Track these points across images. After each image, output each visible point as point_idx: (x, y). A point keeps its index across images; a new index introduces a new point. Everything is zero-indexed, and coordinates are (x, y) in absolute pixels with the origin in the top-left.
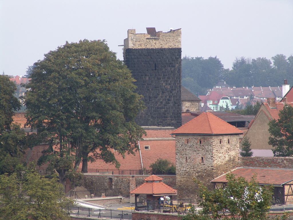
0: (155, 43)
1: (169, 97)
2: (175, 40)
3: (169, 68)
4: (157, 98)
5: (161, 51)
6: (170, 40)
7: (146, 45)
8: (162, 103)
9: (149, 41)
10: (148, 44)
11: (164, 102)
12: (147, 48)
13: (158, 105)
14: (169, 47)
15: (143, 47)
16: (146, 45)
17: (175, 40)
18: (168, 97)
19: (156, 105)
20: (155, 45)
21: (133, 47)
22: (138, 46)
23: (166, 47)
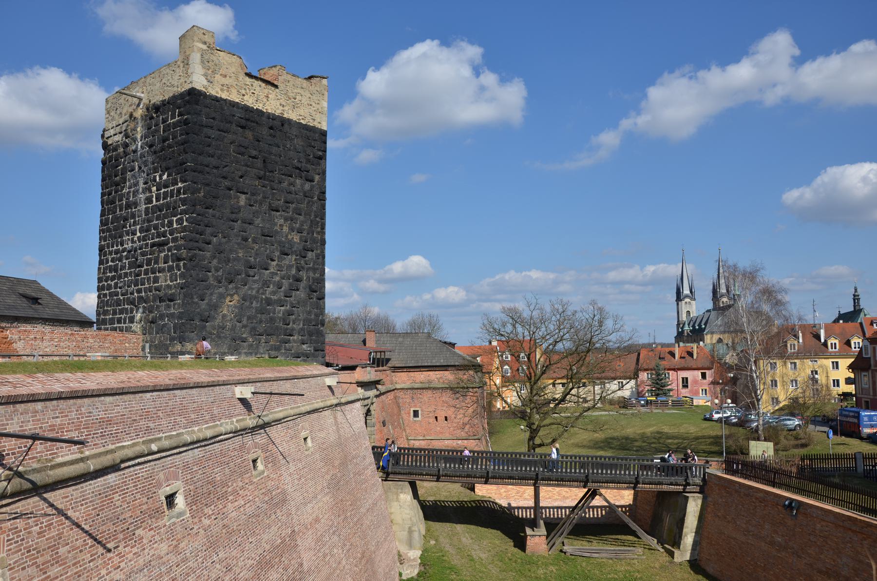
2: (314, 104)
3: (298, 181)
4: (266, 269)
5: (278, 124)
6: (305, 101)
11: (286, 283)
15: (235, 97)
17: (314, 104)
18: (294, 271)
20: (265, 100)
22: (222, 90)
23: (292, 115)
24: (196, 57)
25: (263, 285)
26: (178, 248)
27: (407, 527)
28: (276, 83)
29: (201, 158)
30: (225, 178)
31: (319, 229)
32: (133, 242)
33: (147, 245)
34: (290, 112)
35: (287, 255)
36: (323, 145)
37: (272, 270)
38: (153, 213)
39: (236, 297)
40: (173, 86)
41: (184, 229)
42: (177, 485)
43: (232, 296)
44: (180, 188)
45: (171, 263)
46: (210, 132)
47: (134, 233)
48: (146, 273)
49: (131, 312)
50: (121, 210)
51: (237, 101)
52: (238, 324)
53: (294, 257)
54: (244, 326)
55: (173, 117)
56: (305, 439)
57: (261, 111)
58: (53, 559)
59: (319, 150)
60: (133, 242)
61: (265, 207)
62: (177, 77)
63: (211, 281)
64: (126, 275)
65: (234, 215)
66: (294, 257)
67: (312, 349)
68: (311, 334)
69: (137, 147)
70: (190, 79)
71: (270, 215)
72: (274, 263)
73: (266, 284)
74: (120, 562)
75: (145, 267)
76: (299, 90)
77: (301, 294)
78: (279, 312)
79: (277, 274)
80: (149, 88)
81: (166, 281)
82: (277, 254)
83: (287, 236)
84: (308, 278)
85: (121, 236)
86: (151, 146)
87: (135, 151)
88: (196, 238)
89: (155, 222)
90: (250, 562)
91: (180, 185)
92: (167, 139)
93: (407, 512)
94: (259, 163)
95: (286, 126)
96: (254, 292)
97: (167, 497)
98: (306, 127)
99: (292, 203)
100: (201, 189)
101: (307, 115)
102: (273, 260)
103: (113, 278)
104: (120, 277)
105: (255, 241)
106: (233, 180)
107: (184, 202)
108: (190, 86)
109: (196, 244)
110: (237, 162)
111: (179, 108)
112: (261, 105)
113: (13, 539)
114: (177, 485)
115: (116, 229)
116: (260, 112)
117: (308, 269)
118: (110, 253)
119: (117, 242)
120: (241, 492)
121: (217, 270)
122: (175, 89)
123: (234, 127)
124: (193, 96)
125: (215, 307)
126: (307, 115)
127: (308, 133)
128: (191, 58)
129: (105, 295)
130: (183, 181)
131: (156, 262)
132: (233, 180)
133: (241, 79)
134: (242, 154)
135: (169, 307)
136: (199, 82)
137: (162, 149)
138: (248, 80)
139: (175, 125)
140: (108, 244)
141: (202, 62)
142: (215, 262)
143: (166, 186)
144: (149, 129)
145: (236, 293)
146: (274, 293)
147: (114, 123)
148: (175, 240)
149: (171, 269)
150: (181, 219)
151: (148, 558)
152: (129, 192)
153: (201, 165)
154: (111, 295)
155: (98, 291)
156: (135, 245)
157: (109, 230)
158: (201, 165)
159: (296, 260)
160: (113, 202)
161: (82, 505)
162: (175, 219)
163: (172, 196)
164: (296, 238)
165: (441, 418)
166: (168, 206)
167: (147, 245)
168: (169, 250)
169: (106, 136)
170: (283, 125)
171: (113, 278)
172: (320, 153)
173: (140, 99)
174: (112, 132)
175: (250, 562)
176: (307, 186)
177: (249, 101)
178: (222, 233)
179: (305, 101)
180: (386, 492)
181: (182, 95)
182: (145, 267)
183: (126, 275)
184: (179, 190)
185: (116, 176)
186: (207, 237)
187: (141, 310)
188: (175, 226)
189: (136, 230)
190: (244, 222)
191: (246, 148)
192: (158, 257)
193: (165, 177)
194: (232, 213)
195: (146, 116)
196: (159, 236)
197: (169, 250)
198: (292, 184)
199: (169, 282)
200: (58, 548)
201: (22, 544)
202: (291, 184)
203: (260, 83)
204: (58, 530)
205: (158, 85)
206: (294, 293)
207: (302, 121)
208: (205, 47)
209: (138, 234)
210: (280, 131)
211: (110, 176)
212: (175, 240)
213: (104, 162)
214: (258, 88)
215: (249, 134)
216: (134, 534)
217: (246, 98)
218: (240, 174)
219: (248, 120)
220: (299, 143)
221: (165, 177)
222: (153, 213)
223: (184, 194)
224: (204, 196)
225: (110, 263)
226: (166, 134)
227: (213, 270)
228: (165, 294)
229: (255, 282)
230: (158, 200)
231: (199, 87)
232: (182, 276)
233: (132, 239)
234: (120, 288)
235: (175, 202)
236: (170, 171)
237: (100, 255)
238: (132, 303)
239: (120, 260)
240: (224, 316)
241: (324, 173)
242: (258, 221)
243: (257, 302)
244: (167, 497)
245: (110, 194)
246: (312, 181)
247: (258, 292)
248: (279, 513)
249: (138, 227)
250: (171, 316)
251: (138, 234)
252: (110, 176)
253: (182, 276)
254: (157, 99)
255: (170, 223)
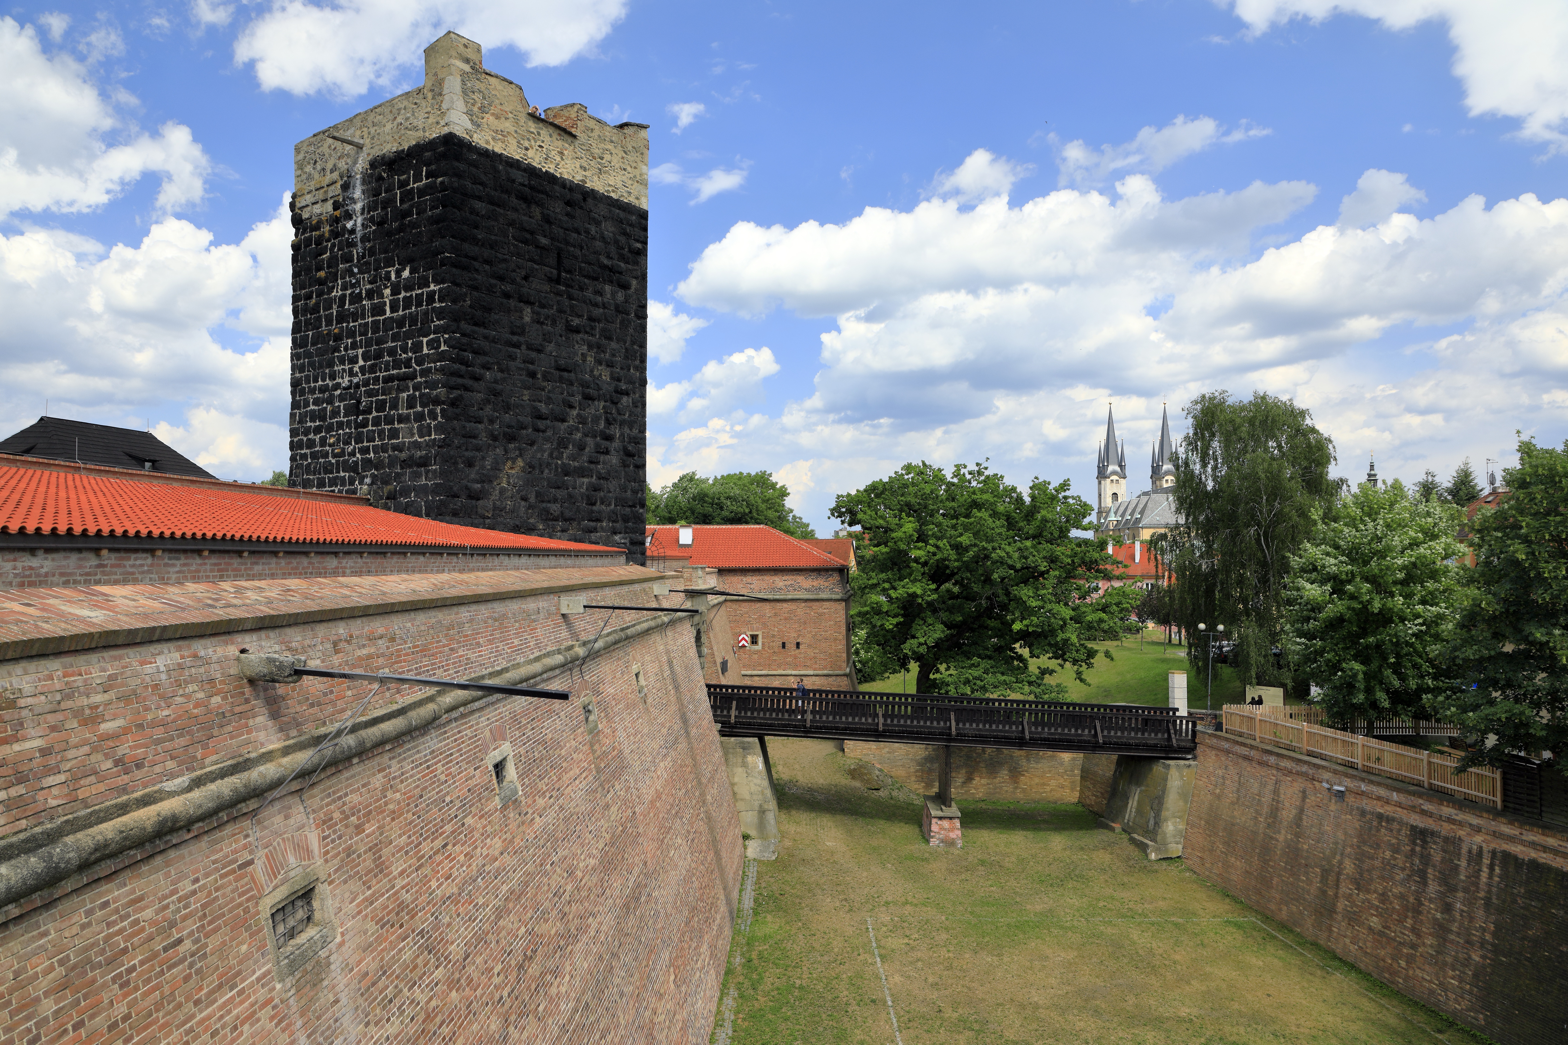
0: (561, 153)
1: (608, 423)
2: (629, 169)
3: (608, 288)
4: (563, 420)
6: (616, 162)
7: (527, 149)
8: (582, 448)
9: (539, 134)
10: (533, 143)
12: (529, 164)
13: (569, 458)
14: (608, 191)
15: (513, 151)
16: (527, 149)
17: (629, 169)
18: (602, 425)
19: (561, 458)
20: (558, 158)
21: (468, 131)
22: (494, 139)
23: (596, 184)
24: (453, 85)
25: (559, 444)
26: (433, 385)
27: (757, 804)
28: (573, 131)
29: (466, 246)
30: (501, 278)
31: (637, 362)
32: (351, 374)
33: (376, 379)
34: (596, 178)
35: (592, 399)
36: (642, 233)
37: (571, 423)
38: (386, 330)
39: (520, 463)
40: (416, 129)
41: (441, 356)
42: (506, 749)
43: (514, 460)
44: (434, 292)
45: (419, 409)
46: (478, 205)
47: (353, 360)
48: (377, 422)
49: (352, 483)
50: (329, 322)
51: (517, 157)
52: (523, 503)
53: (602, 404)
54: (530, 507)
55: (417, 178)
56: (637, 675)
57: (553, 175)
58: (377, 867)
59: (638, 241)
60: (351, 374)
61: (560, 327)
62: (422, 115)
63: (484, 438)
64: (340, 425)
65: (515, 338)
66: (602, 404)
67: (627, 541)
68: (626, 520)
69: (355, 225)
70: (446, 119)
71: (568, 338)
72: (575, 412)
73: (562, 444)
74: (451, 868)
75: (375, 414)
76: (610, 146)
77: (614, 459)
78: (581, 487)
79: (577, 429)
80: (372, 130)
81: (413, 435)
82: (578, 398)
83: (592, 371)
84: (622, 435)
85: (331, 364)
86: (380, 224)
87: (353, 231)
88: (461, 371)
89: (390, 344)
90: (592, 862)
91: (432, 287)
92: (409, 213)
93: (758, 781)
94: (552, 260)
95: (590, 201)
96: (546, 455)
97: (496, 766)
98: (617, 204)
99: (599, 321)
100: (466, 294)
101: (619, 185)
102: (571, 407)
103: (318, 430)
104: (330, 429)
105: (545, 378)
106: (513, 282)
107: (440, 313)
108: (446, 130)
109: (460, 381)
110: (519, 255)
111: (427, 165)
112: (553, 166)
113: (329, 836)
114: (506, 749)
115: (320, 353)
116: (551, 178)
117: (622, 423)
118: (312, 391)
119: (324, 374)
120: (575, 756)
121: (492, 421)
122: (420, 134)
123: (514, 201)
124: (451, 147)
125: (487, 479)
126: (619, 185)
127: (622, 215)
128: (446, 85)
129: (304, 457)
130: (436, 282)
131: (394, 406)
132: (513, 282)
133: (522, 123)
134: (526, 242)
135: (417, 476)
136: (459, 123)
137: (401, 229)
138: (532, 126)
139: (422, 192)
140: (307, 377)
141: (465, 92)
142: (488, 409)
143: (409, 288)
144: (377, 194)
145: (521, 455)
146: (573, 458)
147: (313, 185)
148: (425, 373)
149: (420, 417)
150: (437, 340)
151: (480, 861)
152: (344, 296)
153: (466, 256)
154: (314, 456)
155: (291, 449)
156: (356, 380)
157: (308, 355)
158: (466, 256)
159: (604, 407)
160: (315, 310)
161: (402, 782)
162: (425, 340)
163: (419, 304)
164: (606, 376)
165: (791, 646)
166: (413, 319)
167: (376, 379)
168: (416, 388)
169: (298, 205)
170: (585, 200)
171: (318, 430)
172: (639, 245)
173: (360, 147)
174: (309, 199)
175: (592, 862)
176: (620, 296)
177: (535, 159)
178: (498, 363)
179: (616, 162)
180: (726, 753)
181: (431, 145)
182: (375, 414)
183: (340, 425)
184: (431, 296)
185: (319, 269)
186: (478, 370)
187: (368, 480)
188: (425, 351)
189: (357, 356)
190: (530, 348)
191: (532, 233)
192: (397, 398)
193: (406, 274)
194: (513, 333)
195: (371, 176)
196: (397, 364)
197: (416, 388)
198: (600, 293)
199: (416, 437)
200: (381, 850)
201: (340, 844)
202: (600, 293)
203: (551, 130)
204: (378, 821)
205: (389, 126)
206: (602, 458)
207: (613, 195)
208: (467, 68)
209: (361, 362)
210: (581, 208)
211: (308, 270)
212: (425, 373)
213: (295, 247)
214: (547, 139)
215: (537, 211)
216: (463, 824)
217: (530, 153)
218: (524, 273)
219: (532, 188)
220: (609, 229)
221: (406, 274)
222: (386, 330)
223: (440, 301)
224: (470, 306)
225: (312, 407)
226: (405, 206)
227: (485, 420)
228: (411, 457)
229: (547, 440)
230: (394, 309)
231: (459, 132)
232: (439, 428)
233: (351, 370)
234: (330, 445)
235: (426, 313)
236: (416, 264)
237: (293, 393)
238: (354, 468)
239: (330, 401)
240: (502, 491)
241: (643, 278)
242: (550, 347)
243: (550, 470)
244: (496, 766)
245: (309, 297)
246: (625, 287)
247: (551, 455)
248: (617, 787)
249: (360, 351)
250: (424, 490)
251: (361, 362)
252: (308, 270)
253: (439, 428)
254: (390, 147)
255: (417, 347)
